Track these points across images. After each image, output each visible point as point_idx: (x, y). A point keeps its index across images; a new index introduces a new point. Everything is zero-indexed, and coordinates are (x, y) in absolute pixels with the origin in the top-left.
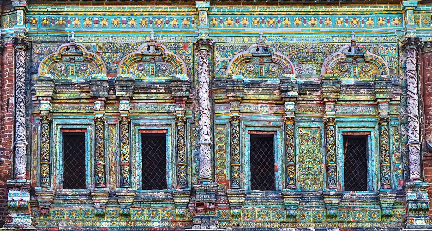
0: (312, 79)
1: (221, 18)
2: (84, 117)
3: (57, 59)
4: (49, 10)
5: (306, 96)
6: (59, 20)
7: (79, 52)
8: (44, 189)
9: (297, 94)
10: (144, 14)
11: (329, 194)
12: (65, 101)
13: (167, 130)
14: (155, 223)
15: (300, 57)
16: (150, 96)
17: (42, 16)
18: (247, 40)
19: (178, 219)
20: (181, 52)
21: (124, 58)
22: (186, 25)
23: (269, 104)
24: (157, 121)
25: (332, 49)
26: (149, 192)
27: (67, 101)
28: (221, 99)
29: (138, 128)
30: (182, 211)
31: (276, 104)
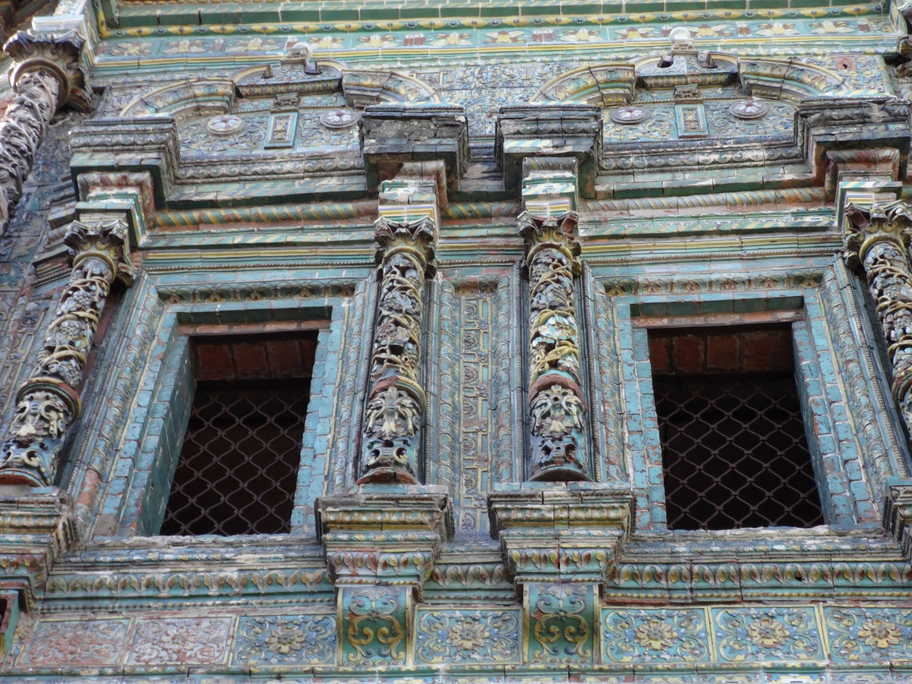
24: (739, 265)
29: (624, 302)
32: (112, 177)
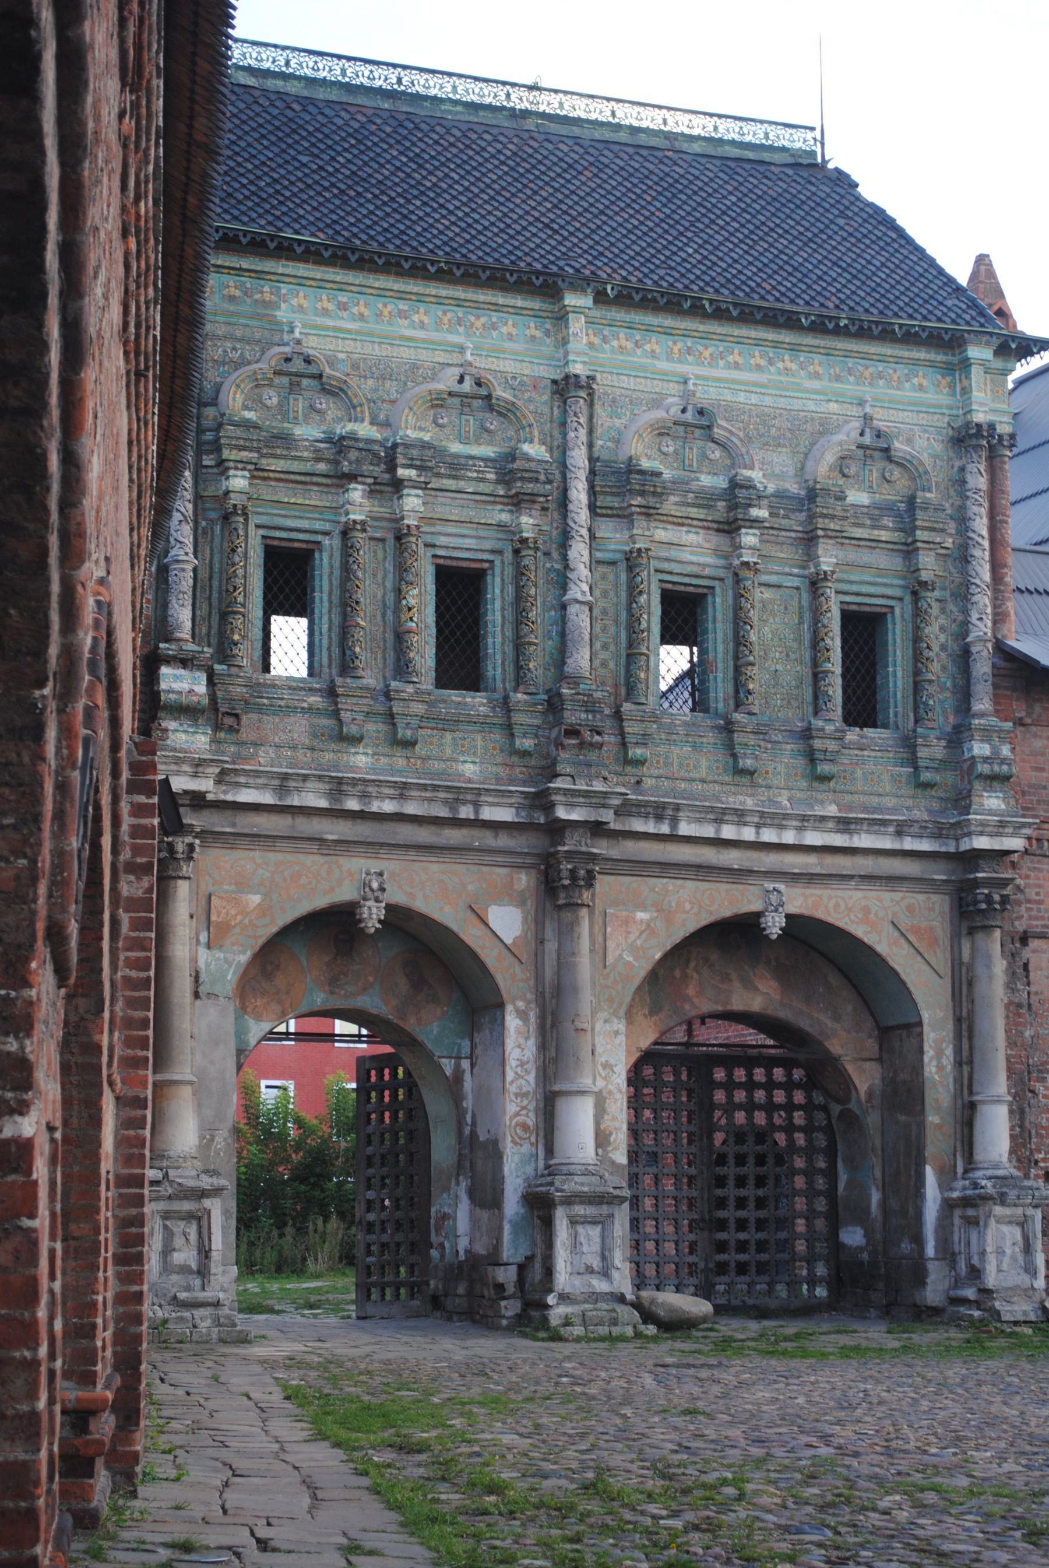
0: (788, 486)
1: (605, 333)
2: (317, 516)
3: (263, 379)
4: (245, 266)
5: (778, 520)
6: (262, 292)
7: (313, 370)
8: (234, 670)
9: (767, 515)
10: (447, 301)
11: (823, 730)
12: (277, 475)
13: (492, 562)
14: (467, 765)
15: (762, 436)
16: (462, 484)
17: (225, 278)
18: (659, 387)
19: (515, 759)
20: (527, 395)
21: (408, 395)
22: (533, 337)
23: (704, 528)
25: (825, 428)
26: (455, 696)
27: (282, 476)
28: (611, 508)
29: (431, 552)
30: (527, 744)
31: (718, 530)
32: (240, 466)
